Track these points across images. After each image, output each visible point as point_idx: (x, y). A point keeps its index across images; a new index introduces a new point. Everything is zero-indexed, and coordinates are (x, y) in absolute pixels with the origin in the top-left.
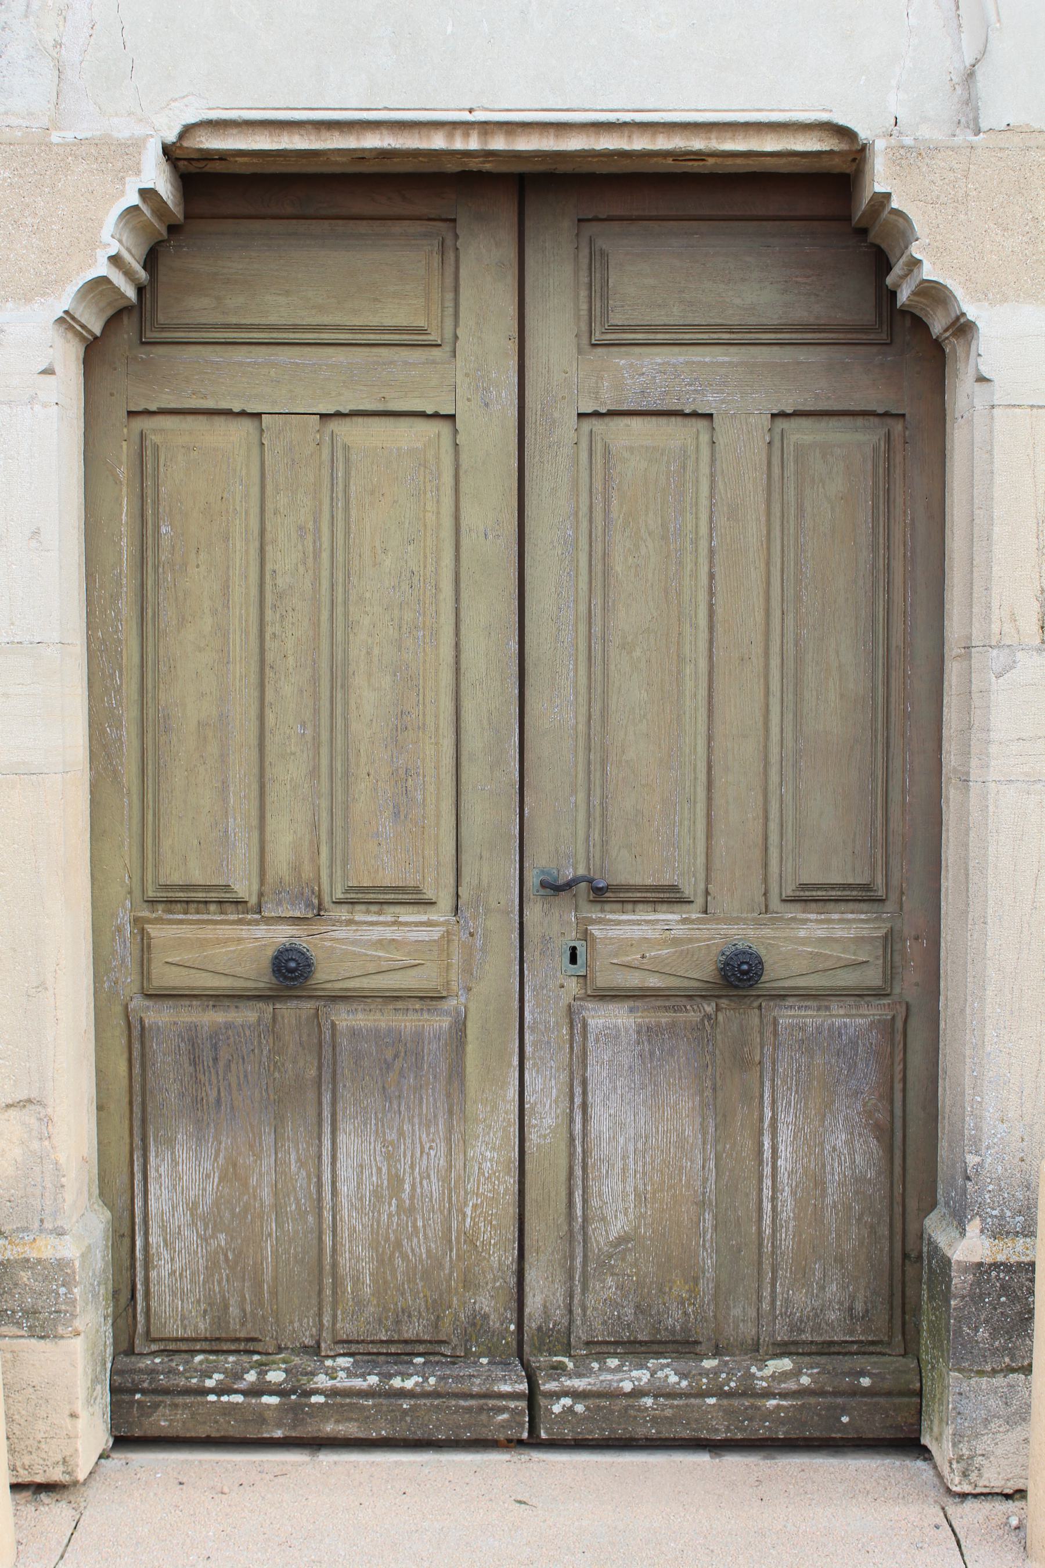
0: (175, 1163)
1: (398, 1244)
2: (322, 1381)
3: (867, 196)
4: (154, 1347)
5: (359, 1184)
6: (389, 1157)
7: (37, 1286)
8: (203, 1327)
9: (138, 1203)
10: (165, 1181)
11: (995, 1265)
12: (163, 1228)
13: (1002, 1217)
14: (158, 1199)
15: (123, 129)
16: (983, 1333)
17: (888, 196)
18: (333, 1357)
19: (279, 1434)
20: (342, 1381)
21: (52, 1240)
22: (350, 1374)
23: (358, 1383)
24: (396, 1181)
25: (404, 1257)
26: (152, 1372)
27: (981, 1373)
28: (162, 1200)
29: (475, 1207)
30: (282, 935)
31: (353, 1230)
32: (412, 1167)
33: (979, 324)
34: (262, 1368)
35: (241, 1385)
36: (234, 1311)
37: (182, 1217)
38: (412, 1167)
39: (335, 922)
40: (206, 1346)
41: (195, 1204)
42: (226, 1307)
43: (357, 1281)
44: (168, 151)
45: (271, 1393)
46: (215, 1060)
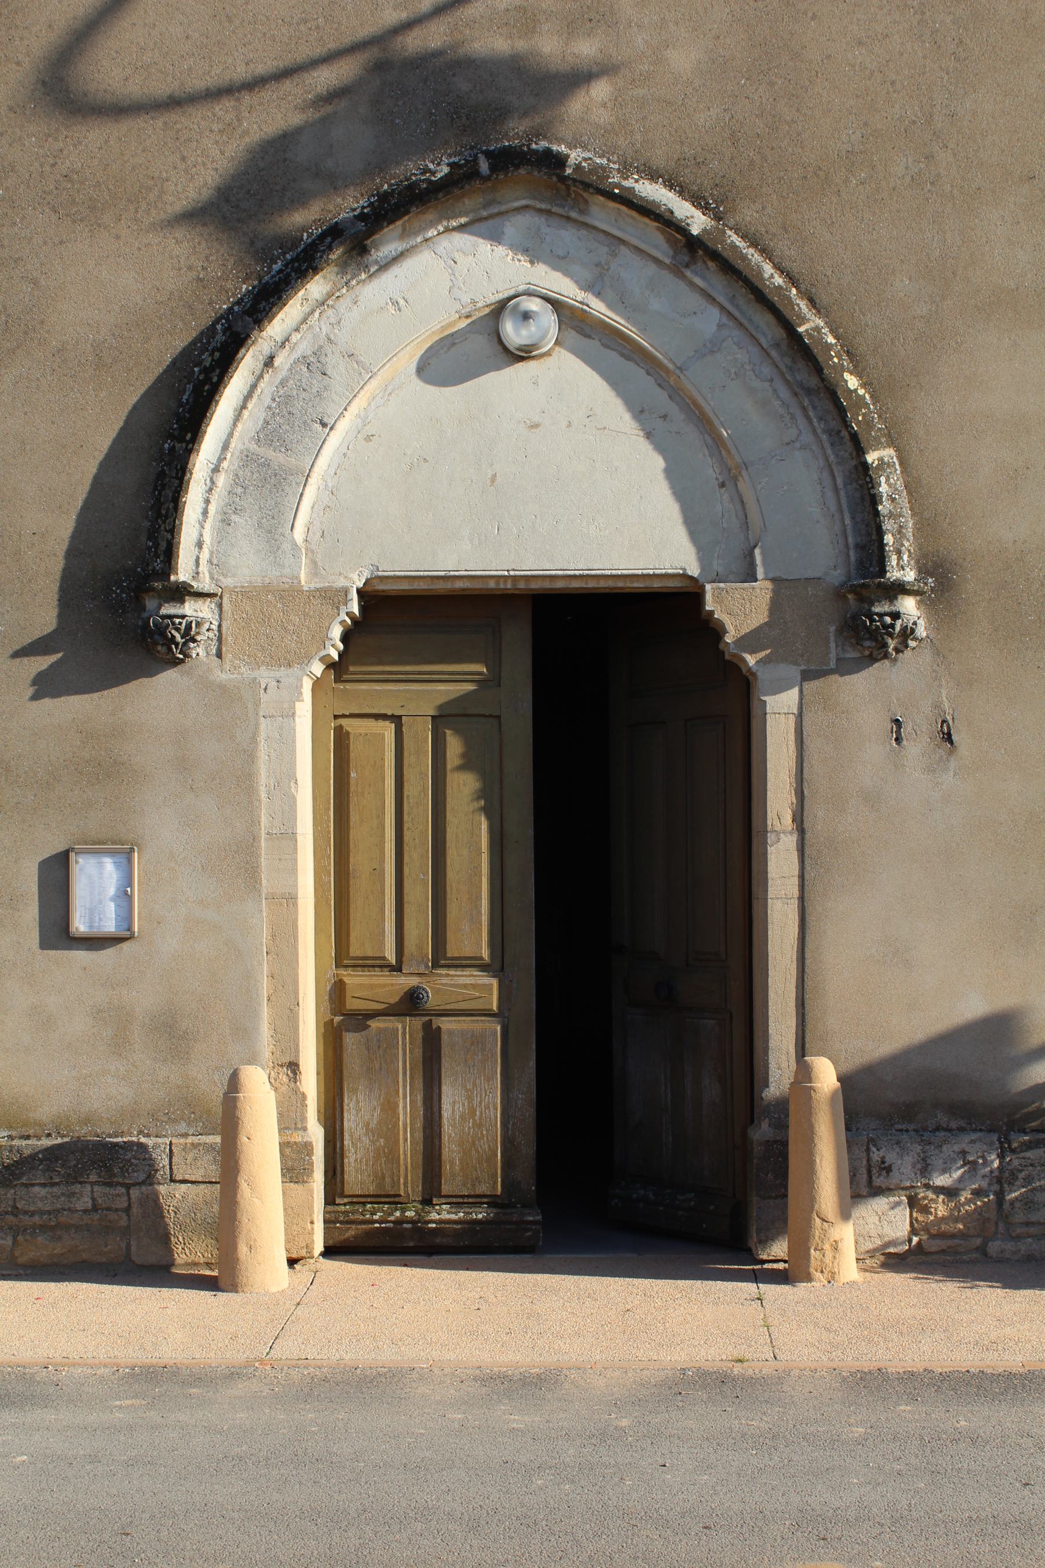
0: (358, 1102)
1: (474, 1144)
2: (434, 1216)
3: (704, 614)
4: (346, 1200)
5: (453, 1111)
6: (470, 1098)
7: (294, 1156)
8: (372, 1189)
9: (338, 1124)
10: (353, 1112)
11: (776, 1142)
12: (351, 1136)
13: (780, 1118)
14: (349, 1120)
15: (341, 583)
17: (712, 612)
18: (440, 1205)
19: (411, 1244)
20: (445, 1216)
21: (300, 1132)
22: (448, 1213)
23: (453, 1217)
24: (472, 1111)
25: (477, 1151)
26: (346, 1213)
27: (770, 1197)
28: (351, 1122)
29: (513, 1124)
30: (414, 981)
31: (450, 1136)
32: (481, 1102)
33: (759, 674)
35: (392, 1218)
36: (388, 1180)
37: (360, 1131)
38: (481, 1102)
39: (441, 975)
40: (373, 1200)
41: (368, 1124)
42: (384, 1178)
43: (452, 1163)
44: (359, 591)
45: (408, 1222)
46: (379, 1047)
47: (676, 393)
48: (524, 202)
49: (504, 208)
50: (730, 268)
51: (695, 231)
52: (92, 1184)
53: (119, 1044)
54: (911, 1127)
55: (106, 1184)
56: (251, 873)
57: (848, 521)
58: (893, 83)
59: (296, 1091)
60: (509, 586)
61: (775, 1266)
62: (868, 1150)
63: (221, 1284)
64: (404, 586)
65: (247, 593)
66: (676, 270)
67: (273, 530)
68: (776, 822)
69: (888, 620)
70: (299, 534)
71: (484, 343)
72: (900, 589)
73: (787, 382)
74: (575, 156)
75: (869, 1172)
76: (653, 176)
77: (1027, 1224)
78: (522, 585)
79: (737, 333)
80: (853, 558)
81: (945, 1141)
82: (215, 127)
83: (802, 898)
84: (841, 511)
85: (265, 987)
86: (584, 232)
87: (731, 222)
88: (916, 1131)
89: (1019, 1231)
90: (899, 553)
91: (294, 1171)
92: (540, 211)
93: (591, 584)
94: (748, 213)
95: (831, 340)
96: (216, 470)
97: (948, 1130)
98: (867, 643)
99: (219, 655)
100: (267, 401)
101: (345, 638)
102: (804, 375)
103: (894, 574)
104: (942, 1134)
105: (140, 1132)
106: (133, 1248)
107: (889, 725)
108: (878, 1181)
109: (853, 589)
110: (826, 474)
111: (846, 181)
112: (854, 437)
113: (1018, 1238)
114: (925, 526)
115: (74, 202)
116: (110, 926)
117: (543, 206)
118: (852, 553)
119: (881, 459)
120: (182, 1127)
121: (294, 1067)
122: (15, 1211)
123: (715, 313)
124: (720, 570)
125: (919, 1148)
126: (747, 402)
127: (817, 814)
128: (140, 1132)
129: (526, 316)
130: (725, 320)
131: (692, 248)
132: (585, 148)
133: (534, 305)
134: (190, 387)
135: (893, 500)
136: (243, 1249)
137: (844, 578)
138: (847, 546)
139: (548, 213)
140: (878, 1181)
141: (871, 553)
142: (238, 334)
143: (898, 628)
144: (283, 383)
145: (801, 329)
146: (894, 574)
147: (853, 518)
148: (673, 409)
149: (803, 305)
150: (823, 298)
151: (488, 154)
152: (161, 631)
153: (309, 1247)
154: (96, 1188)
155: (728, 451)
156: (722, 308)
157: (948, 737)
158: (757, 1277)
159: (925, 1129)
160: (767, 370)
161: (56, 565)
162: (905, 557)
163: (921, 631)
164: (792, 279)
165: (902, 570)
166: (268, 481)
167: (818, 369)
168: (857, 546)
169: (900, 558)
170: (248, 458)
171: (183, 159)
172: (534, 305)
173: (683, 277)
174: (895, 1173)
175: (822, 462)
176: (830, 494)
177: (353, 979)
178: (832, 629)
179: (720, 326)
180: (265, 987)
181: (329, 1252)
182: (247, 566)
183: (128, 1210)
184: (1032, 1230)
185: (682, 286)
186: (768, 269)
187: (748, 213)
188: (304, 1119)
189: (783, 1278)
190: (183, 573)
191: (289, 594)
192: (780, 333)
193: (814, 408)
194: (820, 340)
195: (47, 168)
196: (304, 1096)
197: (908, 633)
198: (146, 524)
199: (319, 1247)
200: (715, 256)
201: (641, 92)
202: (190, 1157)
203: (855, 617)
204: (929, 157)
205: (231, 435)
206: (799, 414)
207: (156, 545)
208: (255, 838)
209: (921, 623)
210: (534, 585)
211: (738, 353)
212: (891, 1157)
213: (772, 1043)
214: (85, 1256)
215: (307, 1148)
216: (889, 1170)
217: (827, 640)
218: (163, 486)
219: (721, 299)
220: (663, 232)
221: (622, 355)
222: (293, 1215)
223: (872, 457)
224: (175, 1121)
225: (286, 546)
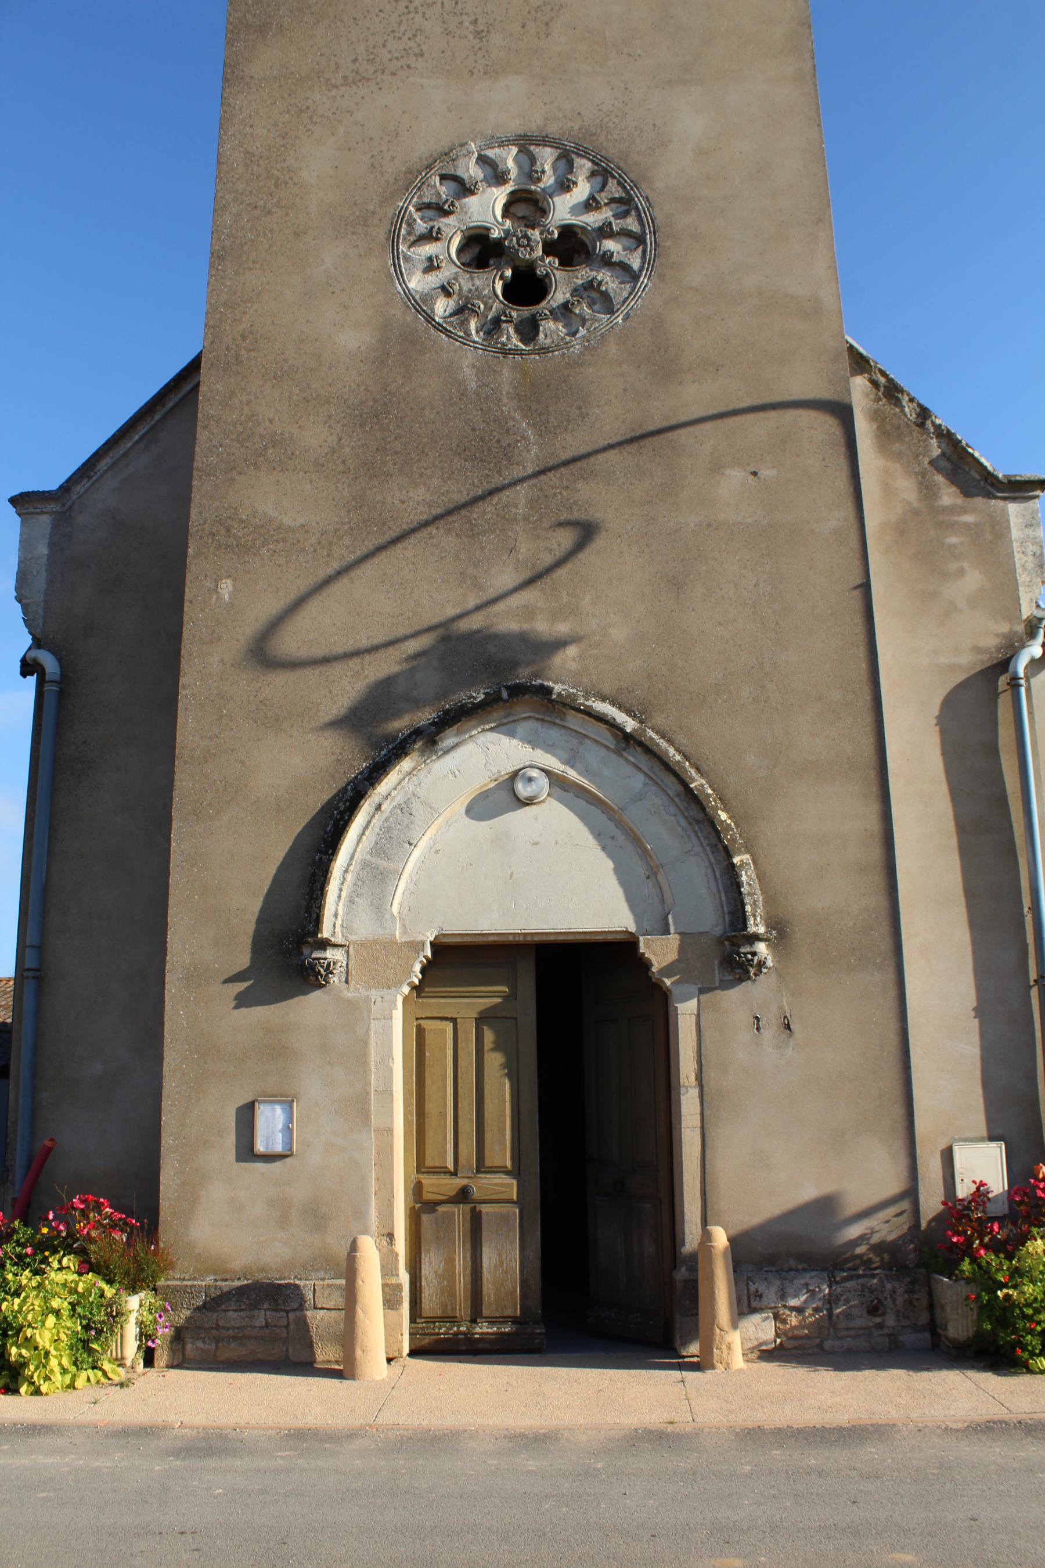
2: (478, 1330)
6: (500, 1255)
8: (439, 1313)
15: (420, 938)
16: (687, 1302)
17: (644, 954)
19: (464, 1348)
23: (490, 1330)
24: (501, 1264)
26: (423, 1328)
28: (426, 1270)
30: (465, 1182)
34: (459, 1327)
36: (449, 1307)
37: (432, 1276)
42: (446, 1305)
44: (431, 943)
47: (619, 823)
48: (528, 714)
49: (516, 718)
50: (649, 751)
51: (628, 730)
52: (266, 1310)
53: (283, 1222)
54: (774, 1269)
55: (274, 1310)
56: (365, 1115)
57: (723, 898)
58: (740, 646)
59: (392, 1251)
60: (521, 939)
61: (692, 1359)
62: (747, 1285)
63: (345, 1374)
64: (459, 940)
65: (364, 945)
66: (618, 752)
67: (379, 907)
68: (686, 1080)
69: (749, 956)
70: (395, 909)
71: (506, 795)
72: (756, 938)
73: (685, 817)
74: (558, 688)
75: (749, 1298)
76: (603, 698)
77: (848, 1329)
78: (529, 938)
79: (654, 788)
80: (727, 920)
81: (795, 1278)
82: (349, 674)
83: (702, 1127)
84: (719, 891)
85: (373, 1186)
86: (563, 731)
87: (650, 724)
88: (777, 1271)
89: (843, 1333)
90: (754, 916)
91: (391, 1302)
92: (538, 719)
93: (571, 938)
94: (659, 720)
95: (710, 791)
96: (346, 871)
97: (797, 1270)
98: (737, 971)
99: (347, 982)
100: (377, 830)
101: (423, 971)
102: (694, 812)
103: (752, 929)
104: (792, 1273)
105: (296, 1277)
106: (290, 1351)
107: (752, 1020)
108: (754, 1304)
109: (728, 939)
110: (709, 870)
111: (716, 700)
112: (726, 848)
113: (842, 1338)
114: (770, 900)
115: (266, 717)
116: (279, 1148)
117: (539, 716)
118: (726, 917)
119: (742, 861)
120: (322, 1274)
121: (391, 1236)
122: (218, 1327)
123: (641, 777)
124: (648, 928)
125: (778, 1282)
126: (662, 828)
127: (711, 1075)
128: (296, 1277)
129: (530, 780)
130: (647, 781)
131: (627, 740)
132: (563, 683)
133: (534, 773)
134: (332, 822)
135: (750, 885)
136: (358, 1352)
137: (721, 932)
138: (723, 912)
139: (542, 720)
140: (754, 1304)
141: (738, 917)
142: (360, 792)
143: (755, 961)
144: (386, 820)
145: (692, 786)
146: (752, 929)
147: (726, 896)
148: (618, 833)
149: (693, 772)
150: (704, 767)
151: (507, 688)
152: (312, 967)
153: (400, 1351)
154: (268, 1313)
155: (651, 857)
156: (646, 774)
157: (788, 1027)
158: (680, 1367)
159: (782, 1270)
160: (672, 809)
161: (251, 928)
162: (758, 919)
163: (770, 963)
164: (686, 757)
165: (757, 926)
166: (377, 877)
167: (703, 808)
168: (730, 913)
169: (755, 919)
170: (365, 864)
171: (330, 692)
172: (534, 773)
173: (622, 756)
174: (765, 1299)
175: (707, 864)
176: (712, 882)
177: (427, 1181)
178: (716, 962)
179: (645, 784)
180: (373, 1186)
181: (414, 1353)
182: (364, 929)
183: (287, 1327)
184: (852, 1333)
185: (622, 761)
186: (672, 751)
187: (659, 720)
188: (397, 1269)
189: (696, 1367)
190: (325, 933)
191: (390, 945)
192: (680, 788)
193: (701, 831)
194: (703, 791)
195: (252, 698)
196: (397, 1255)
197: (761, 964)
198: (304, 903)
199: (406, 1350)
200: (640, 744)
201: (594, 652)
202: (326, 1293)
203: (730, 955)
204: (763, 687)
205: (355, 850)
206: (692, 835)
207: (310, 916)
208: (368, 1094)
209: (769, 958)
210: (536, 939)
211: (655, 800)
212: (762, 1288)
213: (687, 1218)
214: (260, 1356)
215: (399, 1287)
216: (761, 1296)
217: (714, 969)
218: (315, 881)
219: (645, 769)
220: (610, 731)
221: (587, 802)
222: (391, 1330)
223: (736, 860)
224: (317, 1270)
225: (387, 916)
